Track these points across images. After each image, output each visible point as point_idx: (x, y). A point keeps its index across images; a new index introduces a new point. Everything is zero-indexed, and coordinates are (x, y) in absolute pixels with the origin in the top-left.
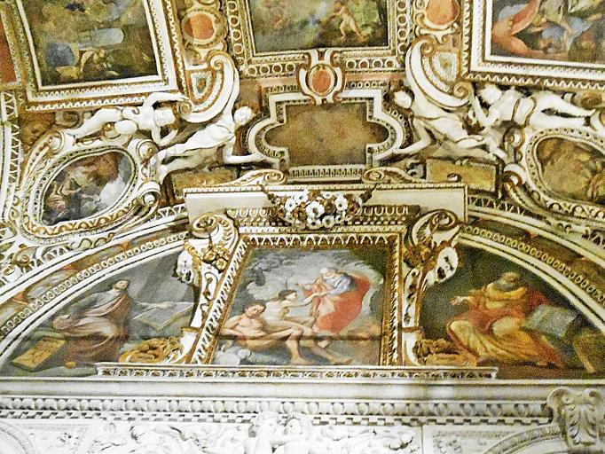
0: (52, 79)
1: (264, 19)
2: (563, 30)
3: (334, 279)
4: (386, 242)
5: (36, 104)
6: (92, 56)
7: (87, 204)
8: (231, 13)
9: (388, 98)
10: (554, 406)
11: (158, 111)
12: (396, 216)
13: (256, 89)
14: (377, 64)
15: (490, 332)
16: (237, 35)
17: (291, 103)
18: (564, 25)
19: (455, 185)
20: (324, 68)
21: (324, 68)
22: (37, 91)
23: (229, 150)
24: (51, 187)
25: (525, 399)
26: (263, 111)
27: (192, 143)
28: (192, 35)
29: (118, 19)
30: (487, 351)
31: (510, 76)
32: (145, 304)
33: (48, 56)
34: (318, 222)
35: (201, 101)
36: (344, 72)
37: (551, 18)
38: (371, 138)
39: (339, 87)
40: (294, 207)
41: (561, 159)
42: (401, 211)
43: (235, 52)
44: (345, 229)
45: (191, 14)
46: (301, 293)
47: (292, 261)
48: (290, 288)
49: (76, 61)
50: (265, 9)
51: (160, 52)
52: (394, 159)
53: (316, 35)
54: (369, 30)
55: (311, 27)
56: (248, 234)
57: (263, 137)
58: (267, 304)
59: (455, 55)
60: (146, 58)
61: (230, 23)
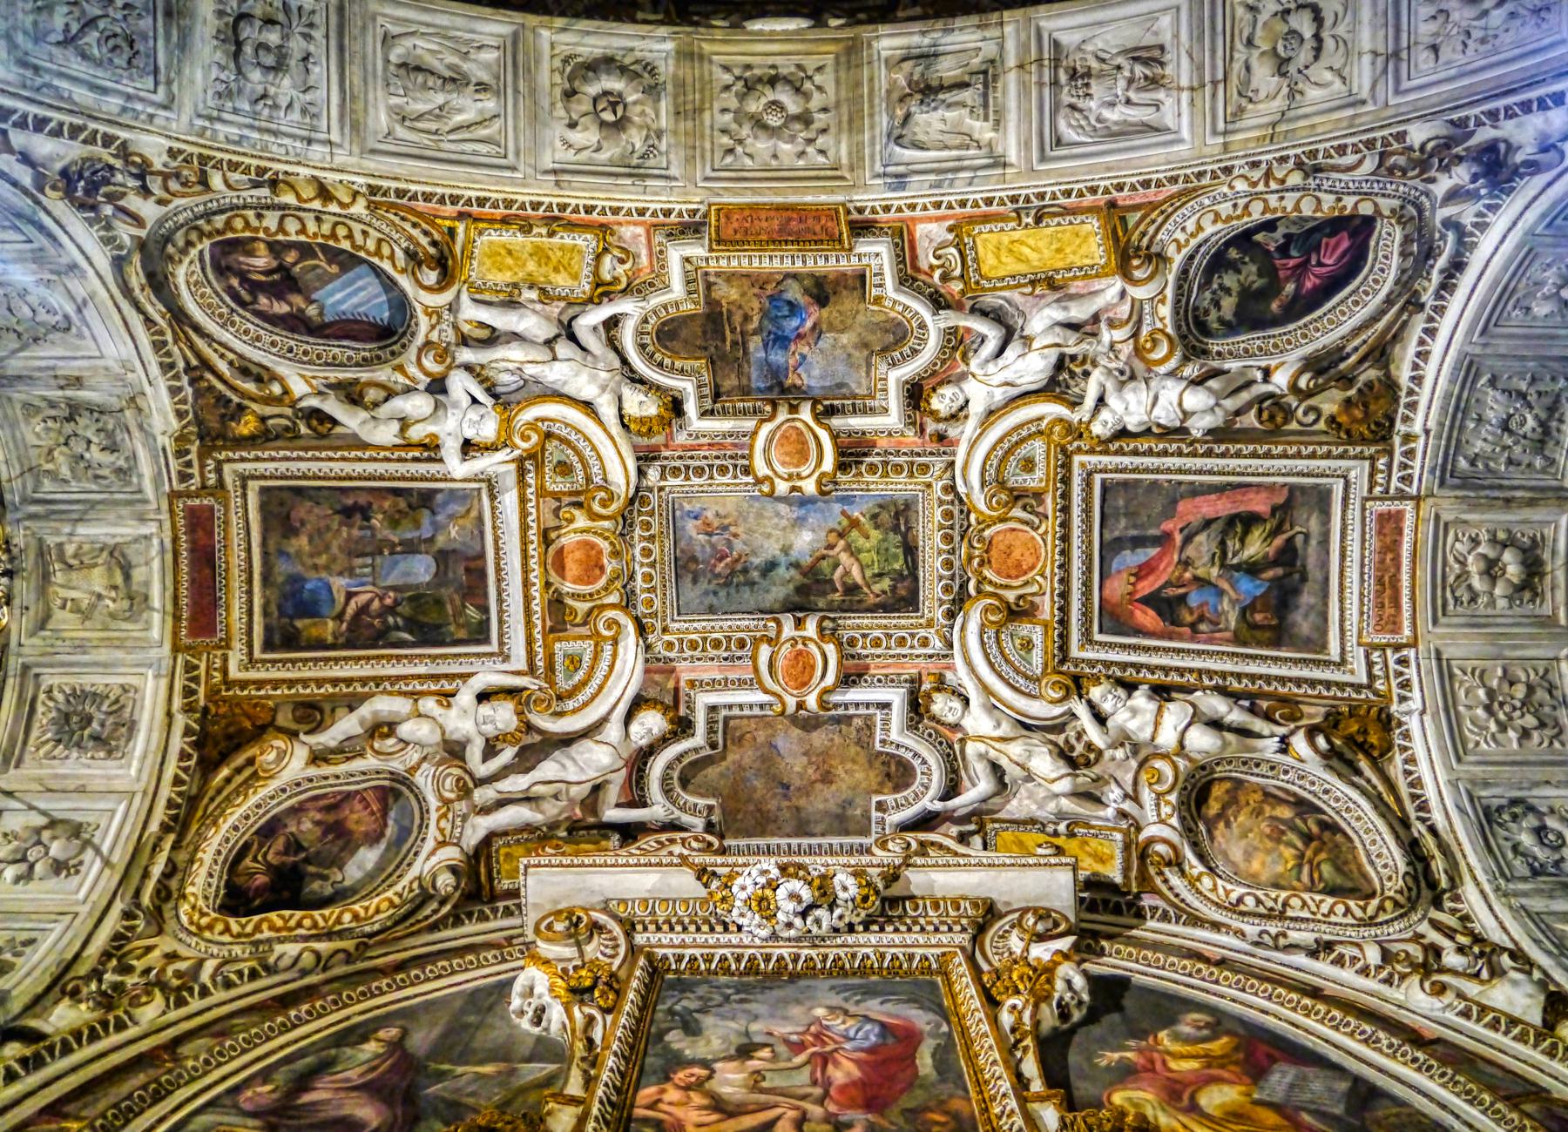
0: (283, 638)
1: (699, 555)
2: (1221, 593)
5: (243, 684)
6: (370, 601)
8: (643, 538)
9: (917, 708)
11: (485, 709)
13: (671, 685)
14: (902, 642)
16: (648, 578)
17: (736, 712)
18: (1225, 586)
23: (613, 793)
24: (246, 847)
26: (682, 727)
27: (548, 769)
31: (1138, 667)
32: (446, 1067)
33: (285, 597)
34: (798, 922)
35: (571, 694)
36: (842, 657)
37: (1200, 572)
39: (830, 679)
40: (750, 889)
41: (1241, 818)
43: (641, 609)
44: (850, 939)
45: (568, 539)
46: (782, 1049)
48: (758, 1039)
49: (338, 608)
51: (500, 601)
52: (926, 821)
54: (886, 584)
55: (781, 571)
57: (676, 775)
60: (472, 612)
61: (638, 557)
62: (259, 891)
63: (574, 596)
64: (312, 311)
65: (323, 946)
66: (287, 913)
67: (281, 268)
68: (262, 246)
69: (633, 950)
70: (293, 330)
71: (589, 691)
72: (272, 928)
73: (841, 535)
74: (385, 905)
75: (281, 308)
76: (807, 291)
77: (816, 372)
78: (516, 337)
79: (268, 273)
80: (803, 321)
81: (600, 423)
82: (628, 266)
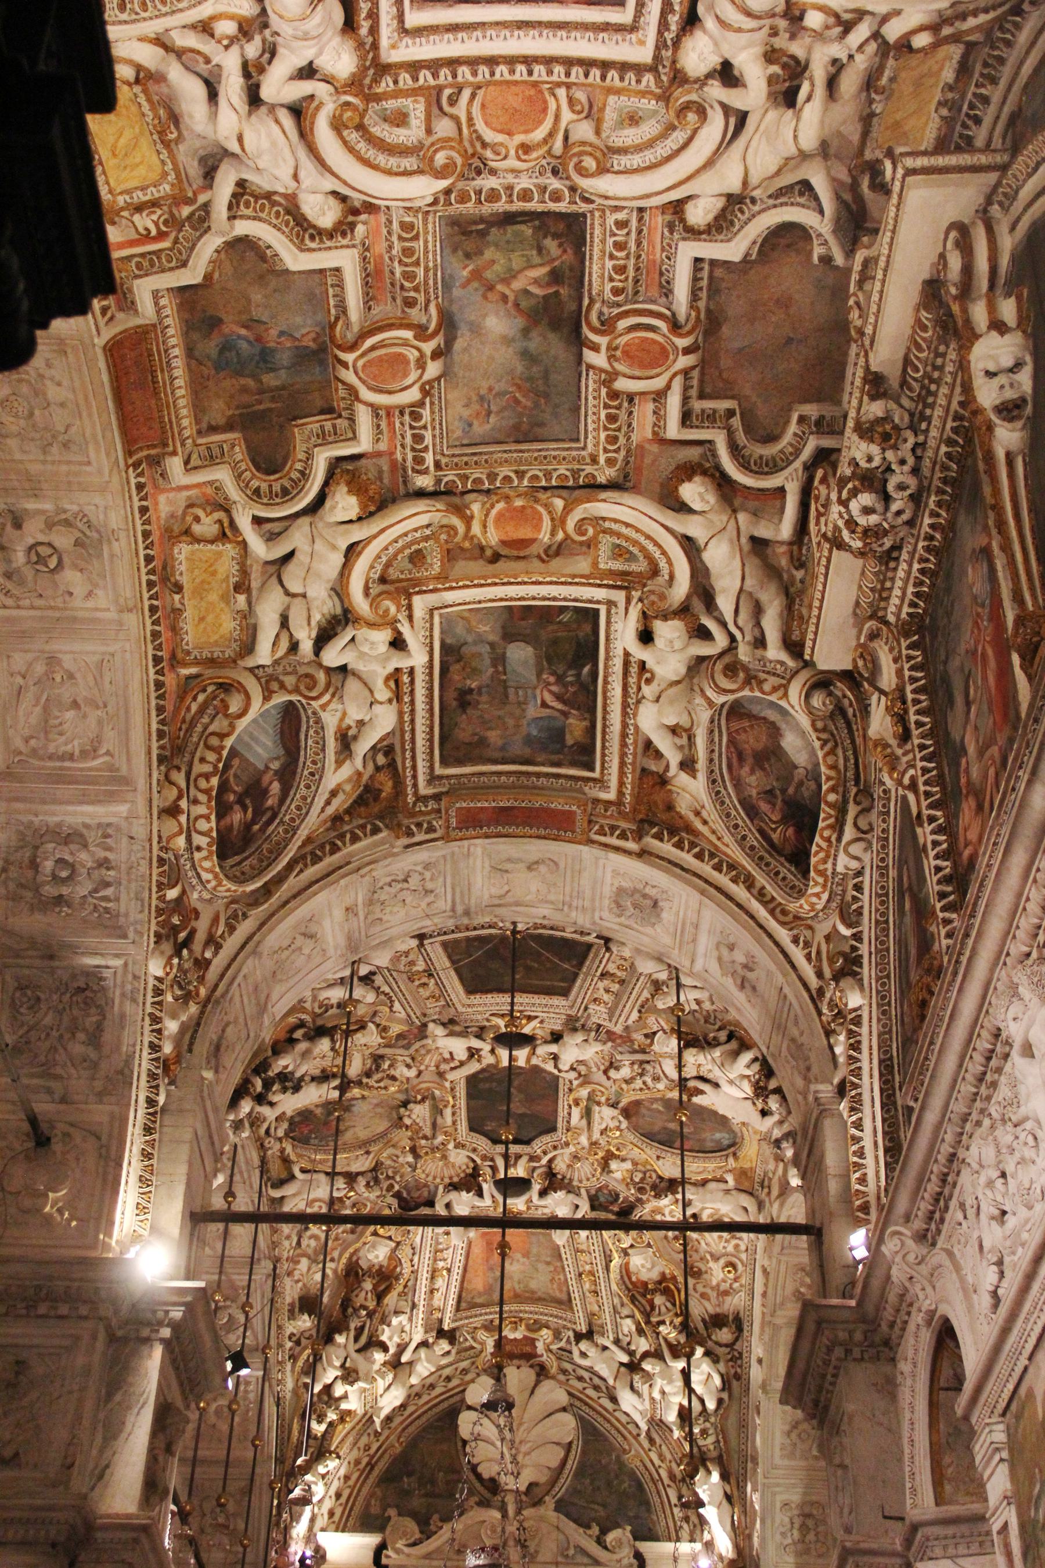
1: (511, 422)
5: (621, 793)
11: (659, 642)
20: (616, 348)
21: (616, 348)
22: (601, 783)
28: (534, 540)
29: (492, 645)
33: (544, 748)
38: (798, 252)
45: (493, 537)
49: (556, 714)
50: (493, 419)
53: (551, 336)
54: (551, 245)
59: (612, 99)
60: (565, 617)
63: (553, 533)
64: (275, 765)
65: (849, 833)
66: (814, 848)
67: (240, 801)
68: (222, 823)
70: (294, 773)
71: (651, 547)
72: (824, 861)
73: (491, 288)
74: (830, 760)
75: (276, 787)
76: (208, 335)
77: (299, 320)
78: (285, 622)
79: (245, 810)
80: (239, 337)
81: (369, 540)
82: (201, 513)
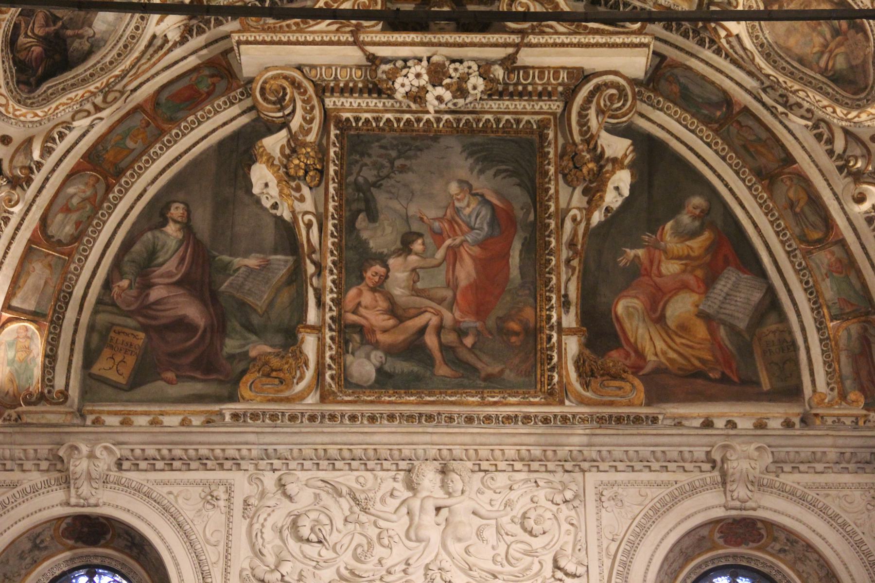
3: (469, 207)
4: (535, 127)
7: (76, 44)
10: (717, 456)
12: (549, 83)
15: (661, 320)
19: (636, 40)
24: (17, 27)
25: (690, 446)
30: (656, 355)
40: (407, 89)
42: (556, 78)
46: (429, 240)
47: (408, 163)
56: (339, 110)
58: (391, 262)
62: (39, 59)
69: (326, 112)
